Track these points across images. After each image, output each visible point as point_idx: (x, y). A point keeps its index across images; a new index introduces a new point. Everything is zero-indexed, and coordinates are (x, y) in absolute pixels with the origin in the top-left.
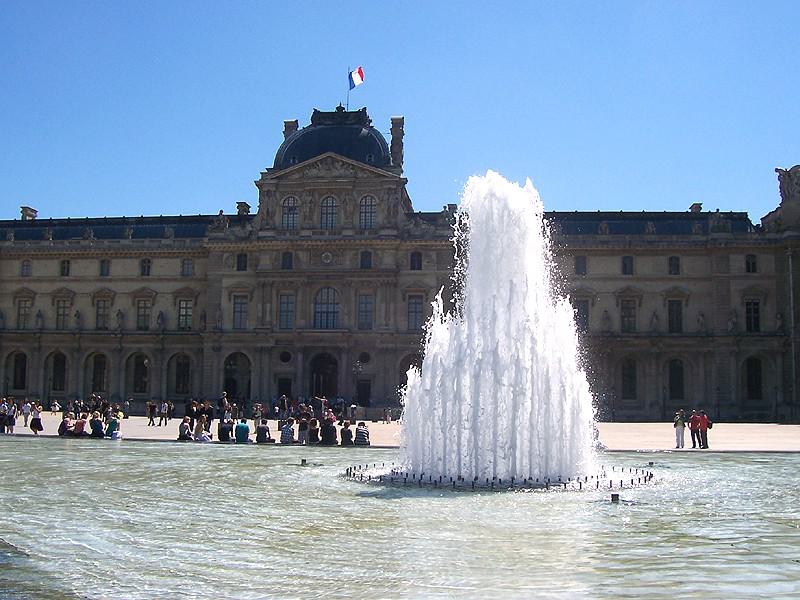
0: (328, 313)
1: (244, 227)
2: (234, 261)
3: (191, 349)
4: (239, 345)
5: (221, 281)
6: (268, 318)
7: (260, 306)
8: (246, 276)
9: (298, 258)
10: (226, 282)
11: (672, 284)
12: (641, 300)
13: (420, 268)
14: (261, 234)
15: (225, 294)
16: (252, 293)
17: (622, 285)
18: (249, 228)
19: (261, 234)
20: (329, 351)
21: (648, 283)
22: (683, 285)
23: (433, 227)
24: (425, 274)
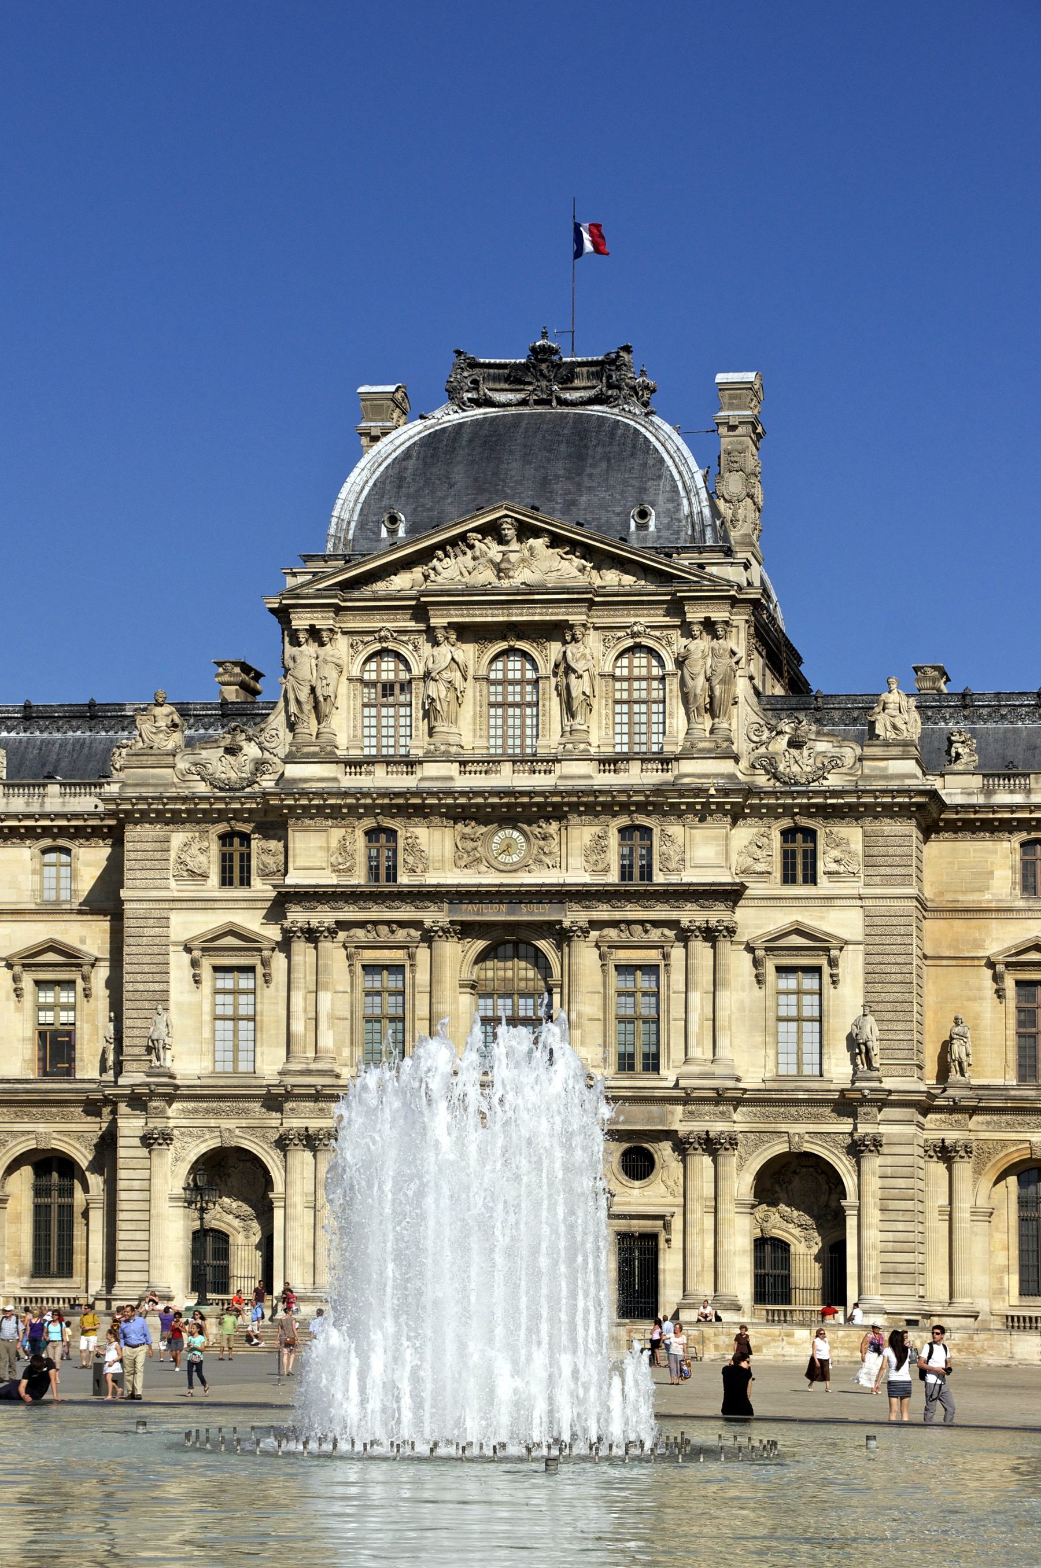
5: (164, 922)
6: (327, 1040)
9: (412, 848)
10: (188, 925)
13: (811, 879)
14: (293, 771)
15: (179, 963)
18: (251, 750)
19: (293, 771)
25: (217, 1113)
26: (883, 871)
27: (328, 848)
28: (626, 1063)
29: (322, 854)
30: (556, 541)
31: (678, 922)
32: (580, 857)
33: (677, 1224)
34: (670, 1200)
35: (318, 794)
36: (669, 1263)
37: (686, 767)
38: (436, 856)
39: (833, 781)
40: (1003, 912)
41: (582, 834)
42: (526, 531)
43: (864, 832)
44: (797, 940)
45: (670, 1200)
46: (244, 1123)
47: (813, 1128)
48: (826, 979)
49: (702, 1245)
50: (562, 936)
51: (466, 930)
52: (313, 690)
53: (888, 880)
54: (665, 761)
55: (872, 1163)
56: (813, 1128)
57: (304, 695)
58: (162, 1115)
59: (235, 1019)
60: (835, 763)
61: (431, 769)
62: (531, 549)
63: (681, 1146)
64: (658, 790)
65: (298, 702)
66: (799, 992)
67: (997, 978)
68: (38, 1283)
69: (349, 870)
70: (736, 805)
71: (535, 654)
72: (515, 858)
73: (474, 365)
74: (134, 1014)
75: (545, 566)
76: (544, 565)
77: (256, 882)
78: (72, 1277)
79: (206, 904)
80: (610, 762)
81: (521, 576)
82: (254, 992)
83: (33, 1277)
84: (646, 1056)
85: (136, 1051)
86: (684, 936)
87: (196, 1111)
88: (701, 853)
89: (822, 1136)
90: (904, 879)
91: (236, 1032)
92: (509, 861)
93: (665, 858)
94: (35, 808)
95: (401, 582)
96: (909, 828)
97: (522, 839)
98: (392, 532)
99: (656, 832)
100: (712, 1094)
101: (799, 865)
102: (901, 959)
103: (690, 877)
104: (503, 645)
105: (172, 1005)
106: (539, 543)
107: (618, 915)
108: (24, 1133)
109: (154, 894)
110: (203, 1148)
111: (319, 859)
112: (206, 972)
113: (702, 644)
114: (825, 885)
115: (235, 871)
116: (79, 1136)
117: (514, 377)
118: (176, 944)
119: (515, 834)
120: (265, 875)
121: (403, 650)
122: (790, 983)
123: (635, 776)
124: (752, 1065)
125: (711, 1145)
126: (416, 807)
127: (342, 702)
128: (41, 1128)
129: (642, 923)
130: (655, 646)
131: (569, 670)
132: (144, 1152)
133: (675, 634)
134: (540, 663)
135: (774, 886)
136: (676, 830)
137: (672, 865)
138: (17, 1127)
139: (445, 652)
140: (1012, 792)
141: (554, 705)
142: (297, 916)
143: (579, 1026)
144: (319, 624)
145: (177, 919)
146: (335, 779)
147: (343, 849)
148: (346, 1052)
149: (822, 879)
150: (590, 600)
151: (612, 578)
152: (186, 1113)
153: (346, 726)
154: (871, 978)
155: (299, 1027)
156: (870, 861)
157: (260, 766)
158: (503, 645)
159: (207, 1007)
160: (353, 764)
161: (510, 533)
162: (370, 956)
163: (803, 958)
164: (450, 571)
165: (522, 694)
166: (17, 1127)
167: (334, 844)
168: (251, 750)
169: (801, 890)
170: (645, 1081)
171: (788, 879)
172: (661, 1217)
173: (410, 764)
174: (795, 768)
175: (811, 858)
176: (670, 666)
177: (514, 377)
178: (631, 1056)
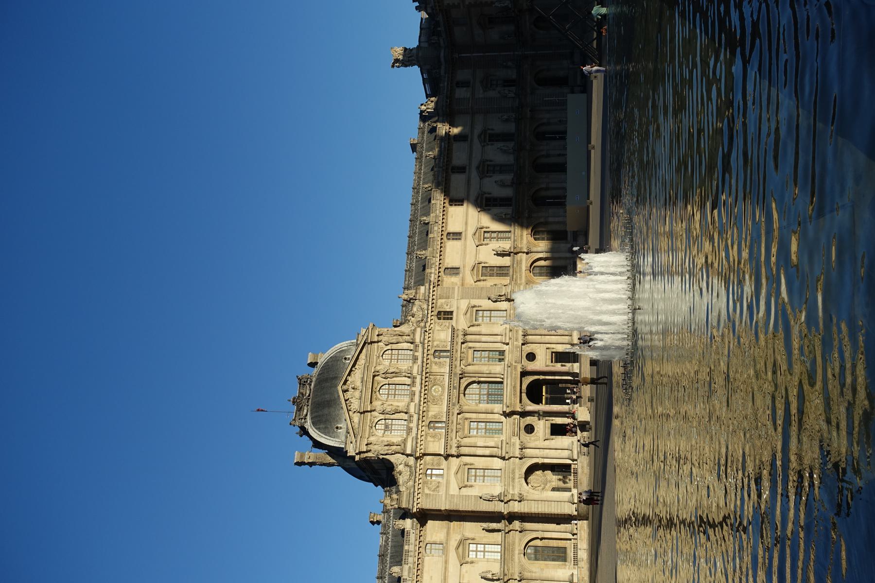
0: (488, 394)
4: (517, 476)
6: (492, 444)
8: (449, 469)
9: (435, 416)
10: (454, 489)
11: (476, 140)
13: (451, 313)
17: (474, 174)
22: (477, 132)
23: (417, 302)
24: (458, 308)
32: (441, 368)
36: (560, 348)
37: (417, 340)
38: (437, 410)
39: (425, 307)
40: (463, 279)
41: (435, 369)
53: (453, 293)
57: (387, 448)
59: (484, 476)
68: (568, 559)
73: (294, 420)
76: (356, 378)
79: (448, 482)
80: (415, 359)
81: (358, 384)
83: (565, 561)
90: (453, 289)
101: (447, 315)
106: (349, 378)
112: (469, 484)
113: (384, 338)
114: (454, 309)
117: (300, 409)
123: (419, 354)
127: (389, 439)
128: (517, 552)
135: (453, 322)
141: (397, 380)
145: (452, 493)
147: (433, 437)
149: (451, 310)
150: (367, 367)
153: (396, 437)
155: (487, 452)
157: (407, 465)
160: (408, 434)
161: (345, 387)
162: (470, 360)
164: (355, 405)
169: (454, 314)
171: (451, 319)
175: (446, 313)
176: (389, 347)
177: (300, 409)
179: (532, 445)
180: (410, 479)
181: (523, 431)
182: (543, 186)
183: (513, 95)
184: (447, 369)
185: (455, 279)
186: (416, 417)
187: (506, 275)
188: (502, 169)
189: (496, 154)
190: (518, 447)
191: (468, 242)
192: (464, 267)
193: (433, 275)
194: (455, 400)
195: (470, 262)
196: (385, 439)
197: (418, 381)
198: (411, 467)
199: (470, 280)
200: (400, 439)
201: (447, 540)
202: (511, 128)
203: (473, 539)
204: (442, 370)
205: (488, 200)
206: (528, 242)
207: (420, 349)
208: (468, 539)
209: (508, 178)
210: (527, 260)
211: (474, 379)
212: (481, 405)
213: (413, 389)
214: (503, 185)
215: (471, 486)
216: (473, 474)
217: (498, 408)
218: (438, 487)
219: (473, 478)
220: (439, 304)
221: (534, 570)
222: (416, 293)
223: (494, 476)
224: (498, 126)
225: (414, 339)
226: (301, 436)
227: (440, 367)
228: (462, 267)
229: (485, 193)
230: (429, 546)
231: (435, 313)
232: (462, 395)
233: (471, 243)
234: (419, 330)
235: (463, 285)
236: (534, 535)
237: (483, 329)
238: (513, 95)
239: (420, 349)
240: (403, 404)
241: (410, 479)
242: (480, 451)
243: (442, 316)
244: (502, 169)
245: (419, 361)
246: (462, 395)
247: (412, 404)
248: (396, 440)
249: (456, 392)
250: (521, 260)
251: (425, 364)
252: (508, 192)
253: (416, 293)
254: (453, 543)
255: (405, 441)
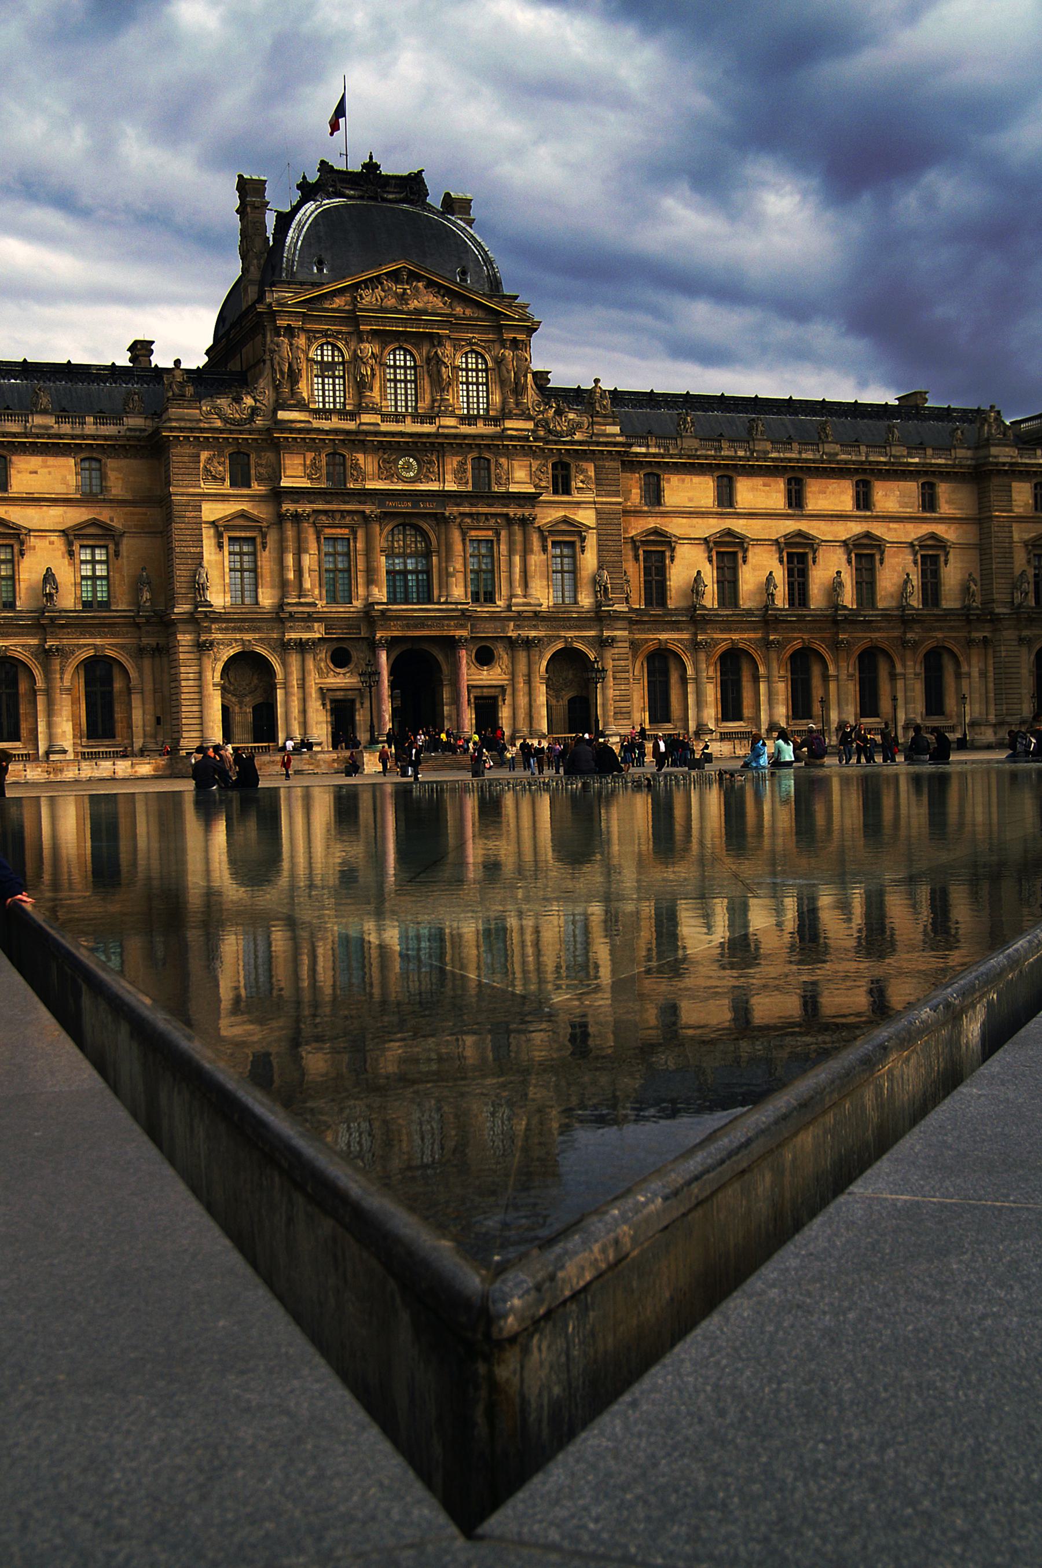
1: (238, 400)
2: (222, 469)
3: (122, 647)
4: (247, 637)
6: (307, 585)
7: (290, 559)
8: (252, 498)
9: (356, 466)
10: (212, 511)
11: (925, 529)
12: (882, 553)
14: (282, 415)
15: (208, 533)
16: (264, 536)
17: (856, 528)
18: (249, 401)
19: (282, 415)
20: (425, 646)
21: (892, 525)
22: (940, 529)
24: (579, 503)
25: (240, 630)
26: (605, 488)
27: (305, 465)
28: (476, 598)
29: (301, 468)
30: (430, 284)
31: (507, 514)
33: (509, 691)
34: (504, 676)
35: (300, 431)
36: (505, 713)
37: (509, 424)
39: (578, 437)
40: (637, 513)
41: (452, 462)
42: (414, 276)
43: (595, 466)
44: (564, 527)
45: (504, 676)
46: (257, 636)
47: (577, 634)
48: (578, 549)
49: (522, 701)
50: (441, 520)
51: (386, 516)
52: (290, 364)
54: (496, 421)
55: (609, 653)
56: (577, 634)
58: (209, 630)
59: (242, 571)
60: (579, 426)
61: (366, 418)
62: (416, 288)
63: (512, 644)
64: (492, 437)
65: (282, 372)
66: (562, 556)
67: (636, 549)
69: (318, 478)
70: (522, 447)
71: (414, 352)
72: (412, 474)
74: (182, 567)
75: (425, 299)
77: (255, 485)
78: (114, 737)
79: (223, 498)
80: (469, 419)
81: (414, 304)
82: (254, 554)
84: (485, 593)
85: (183, 591)
86: (509, 520)
87: (226, 629)
88: (520, 477)
89: (580, 638)
91: (242, 579)
92: (408, 478)
93: (498, 478)
94: (78, 432)
95: (339, 302)
96: (618, 464)
97: (415, 463)
98: (320, 270)
99: (493, 461)
100: (531, 614)
101: (562, 485)
102: (617, 538)
103: (513, 489)
104: (397, 345)
105: (205, 564)
107: (474, 510)
108: (85, 645)
109: (191, 490)
110: (232, 652)
111: (300, 471)
113: (509, 354)
115: (240, 479)
116: (122, 647)
118: (206, 522)
119: (411, 460)
120: (260, 480)
121: (339, 344)
122: (558, 551)
123: (481, 428)
124: (543, 596)
125: (528, 644)
126: (358, 441)
128: (98, 641)
129: (486, 514)
130: (483, 352)
131: (439, 362)
132: (197, 655)
133: (497, 346)
134: (417, 357)
136: (503, 460)
137: (503, 482)
138: (82, 641)
139: (369, 348)
140: (640, 446)
142: (288, 507)
143: (453, 575)
144: (293, 324)
146: (309, 422)
148: (317, 592)
149: (575, 492)
151: (459, 310)
152: (220, 630)
154: (601, 549)
156: (599, 482)
157: (254, 411)
158: (397, 345)
159: (226, 564)
160: (316, 411)
163: (567, 538)
164: (368, 298)
165: (405, 374)
166: (82, 641)
167: (308, 462)
168: (249, 401)
170: (489, 608)
172: (502, 686)
173: (352, 416)
174: (558, 428)
178: (477, 593)
179: (310, 665)
180: (226, 420)
181: (335, 645)
182: (832, 671)
183: (1017, 601)
184: (451, 486)
185: (636, 495)
186: (351, 426)
187: (648, 602)
188: (866, 583)
189: (896, 572)
190: (305, 636)
191: (713, 521)
192: (665, 514)
193: (643, 450)
194: (391, 506)
195: (676, 527)
196: (304, 366)
197: (427, 428)
198: (251, 419)
199: (637, 527)
200: (305, 395)
201: (111, 501)
202: (950, 601)
203: (117, 554)
204: (449, 477)
205: (802, 558)
206: (716, 642)
207: (490, 430)
208: (117, 545)
209: (848, 598)
210: (679, 640)
211: (434, 542)
212: (383, 559)
213: (408, 420)
214: (836, 586)
215: (220, 546)
216: (245, 549)
217: (380, 594)
218: (214, 478)
219: (237, 549)
220: (585, 465)
221: (67, 677)
222: (605, 416)
223: (242, 591)
224: (953, 573)
225: (509, 416)
226: (299, 187)
227: (455, 473)
228: (662, 508)
229: (815, 551)
230: (95, 465)
231: (567, 459)
232: (400, 520)
233: (712, 527)
234: (530, 425)
235: (626, 512)
236: (133, 674)
237: (536, 559)
238: (1017, 601)
239: (490, 430)
240: (378, 400)
241: (226, 420)
242: (290, 559)
243: (560, 472)
244: (866, 583)
245: (465, 429)
246: (400, 520)
247: (377, 419)
248: (303, 387)
249: (406, 507)
250: (679, 630)
251: (458, 444)
252: (817, 598)
253: (605, 416)
254: (104, 515)
255: (302, 406)
